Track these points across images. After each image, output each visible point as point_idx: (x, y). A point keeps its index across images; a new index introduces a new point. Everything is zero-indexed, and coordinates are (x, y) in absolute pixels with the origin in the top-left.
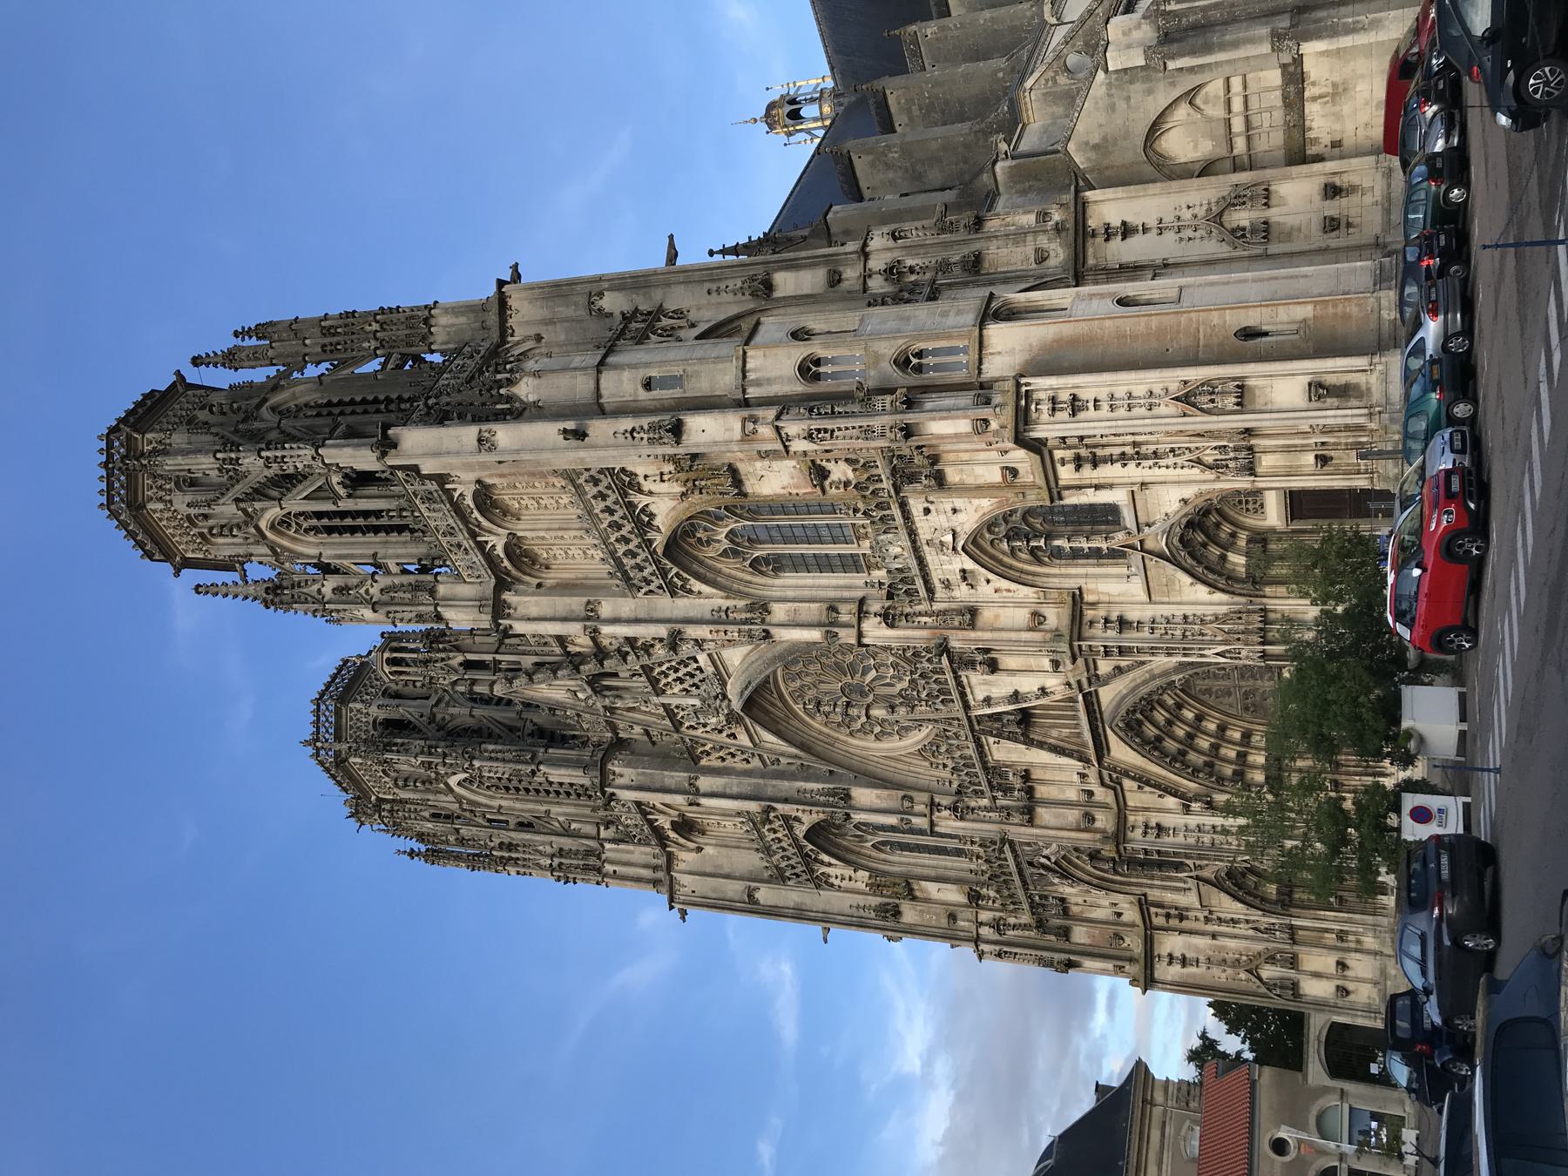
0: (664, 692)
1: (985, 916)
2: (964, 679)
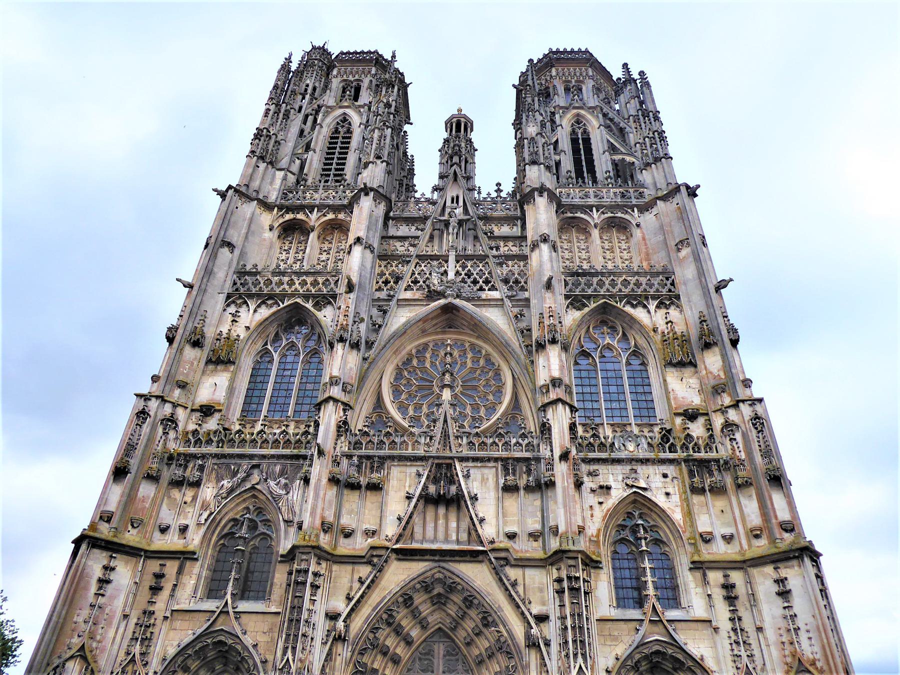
0: (457, 262)
1: (181, 414)
2: (492, 464)
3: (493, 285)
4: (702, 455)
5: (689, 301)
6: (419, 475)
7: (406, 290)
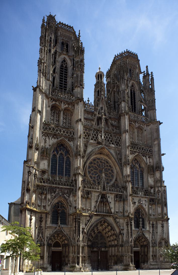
0: (104, 133)
3: (113, 143)
4: (153, 197)
5: (155, 157)
6: (98, 196)
7: (91, 139)
